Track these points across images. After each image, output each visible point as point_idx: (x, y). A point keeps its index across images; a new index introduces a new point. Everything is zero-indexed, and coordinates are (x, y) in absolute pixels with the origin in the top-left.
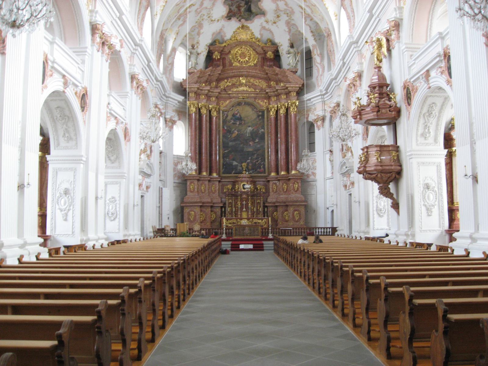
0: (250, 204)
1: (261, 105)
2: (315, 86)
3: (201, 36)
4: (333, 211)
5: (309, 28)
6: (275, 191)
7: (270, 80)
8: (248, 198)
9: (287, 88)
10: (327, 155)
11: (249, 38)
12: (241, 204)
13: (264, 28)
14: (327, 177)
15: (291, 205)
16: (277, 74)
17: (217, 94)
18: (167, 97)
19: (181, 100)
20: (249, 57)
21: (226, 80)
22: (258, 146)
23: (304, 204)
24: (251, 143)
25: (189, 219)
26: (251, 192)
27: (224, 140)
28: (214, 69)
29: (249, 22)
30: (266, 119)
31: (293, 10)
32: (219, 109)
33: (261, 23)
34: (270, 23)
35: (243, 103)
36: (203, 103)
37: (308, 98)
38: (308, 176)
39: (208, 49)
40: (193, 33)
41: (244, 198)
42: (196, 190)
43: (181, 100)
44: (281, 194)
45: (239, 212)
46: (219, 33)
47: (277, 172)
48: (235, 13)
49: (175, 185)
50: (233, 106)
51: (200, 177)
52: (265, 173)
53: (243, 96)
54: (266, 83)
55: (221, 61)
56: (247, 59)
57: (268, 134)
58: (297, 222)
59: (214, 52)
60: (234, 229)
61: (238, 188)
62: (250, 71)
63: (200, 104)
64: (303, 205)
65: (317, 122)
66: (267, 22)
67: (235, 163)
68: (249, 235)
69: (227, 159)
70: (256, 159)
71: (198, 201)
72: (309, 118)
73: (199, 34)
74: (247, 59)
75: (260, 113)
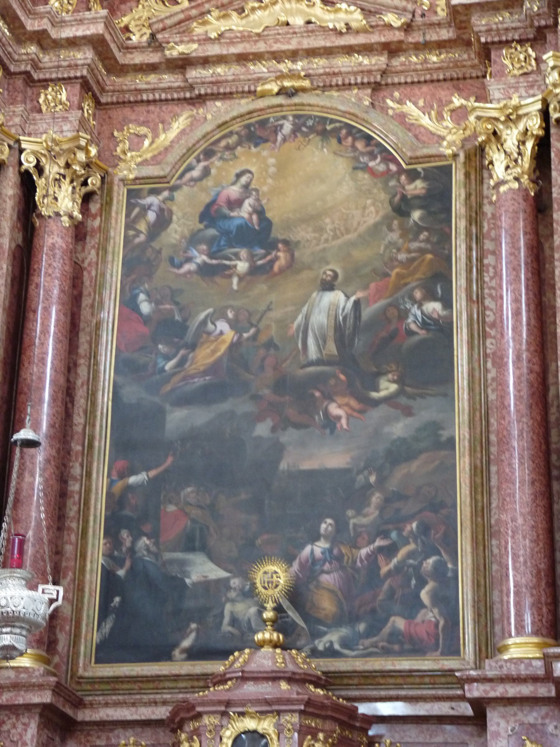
24: (334, 410)
35: (288, 127)
50: (208, 154)
53: (281, 76)
69: (144, 541)
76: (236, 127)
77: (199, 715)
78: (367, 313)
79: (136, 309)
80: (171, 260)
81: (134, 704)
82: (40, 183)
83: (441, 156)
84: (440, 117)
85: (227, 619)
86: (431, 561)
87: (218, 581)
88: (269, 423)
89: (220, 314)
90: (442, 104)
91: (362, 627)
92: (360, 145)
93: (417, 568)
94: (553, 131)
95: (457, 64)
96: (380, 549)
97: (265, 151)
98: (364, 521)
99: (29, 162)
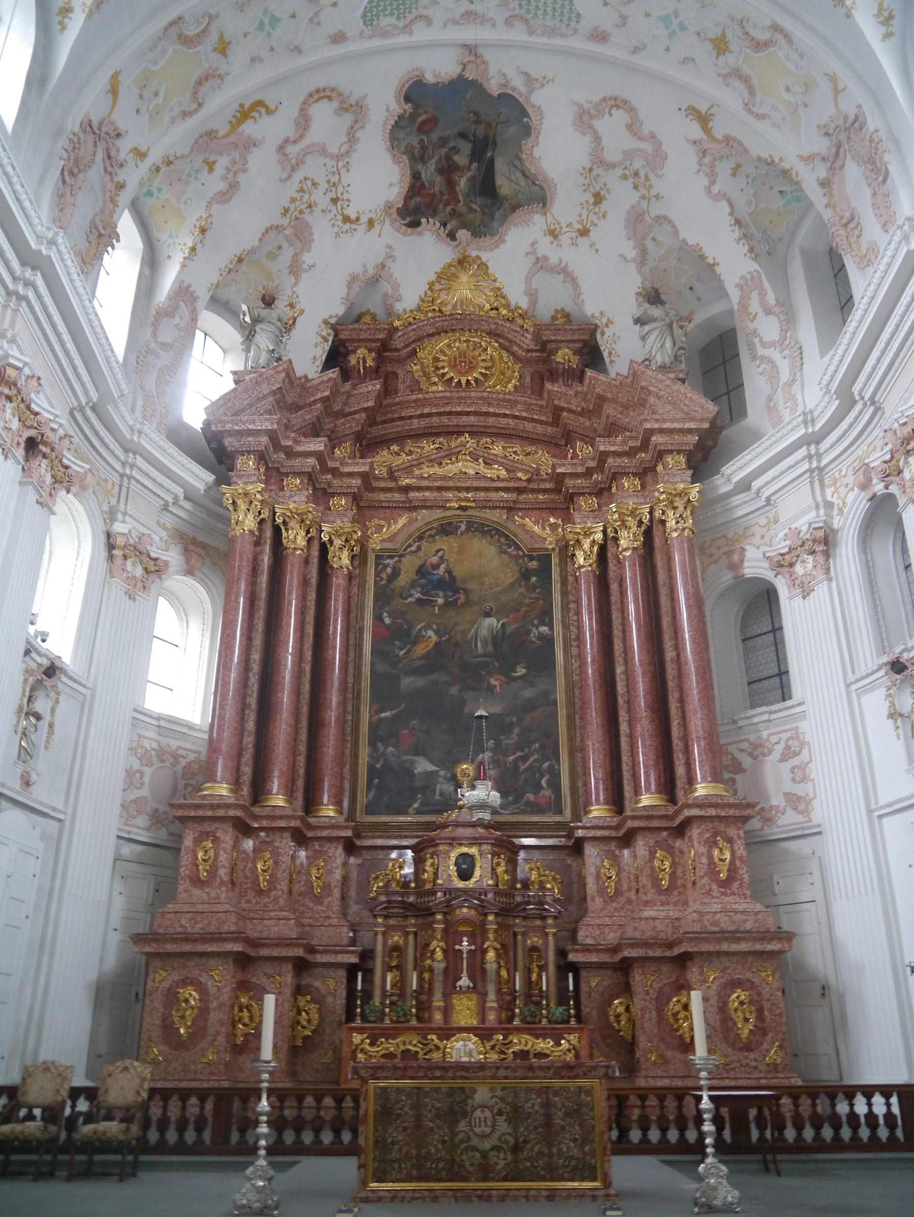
0: (491, 955)
3: (304, 277)
5: (728, 210)
6: (611, 891)
8: (483, 924)
10: (865, 699)
11: (487, 307)
12: (445, 952)
13: (540, 264)
14: (882, 802)
17: (356, 482)
18: (126, 451)
19: (201, 487)
21: (395, 448)
22: (528, 693)
24: (493, 682)
25: (168, 1028)
26: (497, 893)
27: (382, 667)
28: (348, 386)
29: (487, 240)
30: (556, 586)
31: (658, 144)
33: (533, 244)
34: (565, 239)
35: (463, 527)
36: (291, 506)
37: (735, 479)
39: (331, 339)
41: (466, 921)
42: (223, 873)
44: (646, 903)
45: (438, 995)
46: (374, 280)
47: (617, 801)
48: (434, 195)
49: (127, 850)
50: (420, 538)
53: (461, 500)
59: (354, 352)
60: (369, 1106)
62: (492, 410)
65: (791, 565)
66: (553, 234)
67: (423, 766)
68: (500, 1161)
71: (226, 928)
72: (746, 564)
73: (296, 269)
75: (534, 564)
77: (438, 844)
78: (509, 630)
80: (401, 595)
81: (389, 837)
82: (331, 549)
83: (547, 549)
84: (544, 528)
86: (546, 764)
87: (432, 772)
89: (428, 627)
90: (544, 522)
91: (511, 798)
92: (502, 540)
93: (540, 768)
95: (552, 501)
96: (519, 757)
97: (451, 539)
98: (511, 742)
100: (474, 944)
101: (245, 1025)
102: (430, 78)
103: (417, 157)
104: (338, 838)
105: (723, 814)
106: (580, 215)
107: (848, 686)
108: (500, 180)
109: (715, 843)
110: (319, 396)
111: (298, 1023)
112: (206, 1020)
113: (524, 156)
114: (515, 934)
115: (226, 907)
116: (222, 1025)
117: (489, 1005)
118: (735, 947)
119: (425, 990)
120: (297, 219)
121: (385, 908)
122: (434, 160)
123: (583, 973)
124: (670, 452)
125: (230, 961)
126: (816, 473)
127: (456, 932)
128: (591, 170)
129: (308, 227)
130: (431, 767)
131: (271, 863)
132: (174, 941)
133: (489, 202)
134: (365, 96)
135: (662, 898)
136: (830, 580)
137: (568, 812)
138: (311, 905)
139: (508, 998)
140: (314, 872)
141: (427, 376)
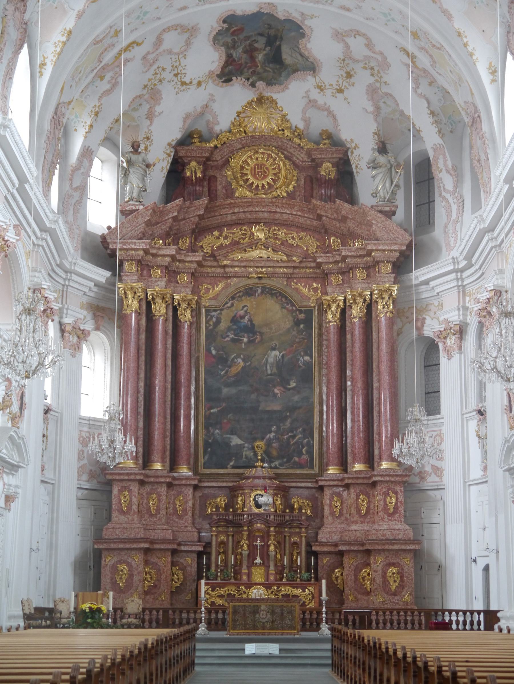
0: (272, 547)
1: (302, 296)
2: (440, 249)
3: (156, 121)
4: (487, 569)
5: (426, 105)
6: (337, 514)
7: (326, 232)
8: (268, 532)
9: (369, 253)
12: (248, 546)
13: (312, 103)
14: (472, 478)
15: (379, 551)
16: (344, 219)
18: (66, 272)
19: (103, 280)
20: (275, 174)
21: (216, 233)
22: (296, 398)
23: (412, 547)
24: (276, 391)
28: (187, 203)
29: (276, 88)
30: (315, 331)
32: (198, 303)
33: (307, 92)
34: (328, 92)
35: (259, 291)
36: (157, 288)
38: (422, 476)
39: (172, 154)
40: (135, 114)
41: (259, 530)
42: (135, 508)
43: (103, 280)
44: (353, 522)
46: (202, 114)
47: (344, 465)
48: (241, 65)
49: (79, 494)
50: (233, 298)
51: (147, 476)
52: (312, 467)
53: (258, 273)
54: (317, 240)
55: (206, 184)
56: (269, 179)
57: (320, 369)
58: (395, 594)
59: (189, 163)
61: (244, 505)
62: (278, 210)
63: (149, 291)
64: (410, 550)
65: (445, 338)
66: (321, 88)
67: (236, 441)
68: (268, 625)
70: (291, 430)
71: (139, 536)
72: (425, 328)
73: (150, 116)
74: (271, 182)
75: (302, 316)
76: (242, 289)
78: (286, 359)
79: (211, 353)
83: (311, 307)
85: (244, 456)
86: (306, 440)
87: (241, 444)
88: (256, 394)
89: (238, 356)
91: (285, 460)
92: (283, 300)
93: (302, 443)
94: (347, 307)
95: (315, 273)
96: (290, 436)
97: (252, 299)
98: (286, 427)
99: (176, 303)
100: (263, 541)
101: (148, 581)
102: (239, 13)
103: (230, 47)
104: (190, 485)
105: (393, 480)
106: (338, 81)
107: (463, 415)
108: (284, 56)
109: (388, 494)
110: (171, 215)
111: (173, 580)
112: (132, 580)
113: (301, 47)
114: (285, 536)
115: (138, 525)
116: (140, 582)
117: (270, 572)
118: (391, 547)
119: (238, 564)
120: (152, 89)
121: (217, 523)
122: (241, 47)
123: (320, 556)
124: (383, 262)
125: (143, 552)
126: (461, 288)
127: (254, 536)
128: (344, 60)
129: (159, 92)
130: (240, 442)
131: (156, 500)
132: (115, 542)
133: (278, 67)
134: (198, 24)
135: (362, 519)
136: (461, 353)
137: (316, 470)
138: (177, 520)
139: (280, 568)
140: (178, 503)
141: (235, 178)
